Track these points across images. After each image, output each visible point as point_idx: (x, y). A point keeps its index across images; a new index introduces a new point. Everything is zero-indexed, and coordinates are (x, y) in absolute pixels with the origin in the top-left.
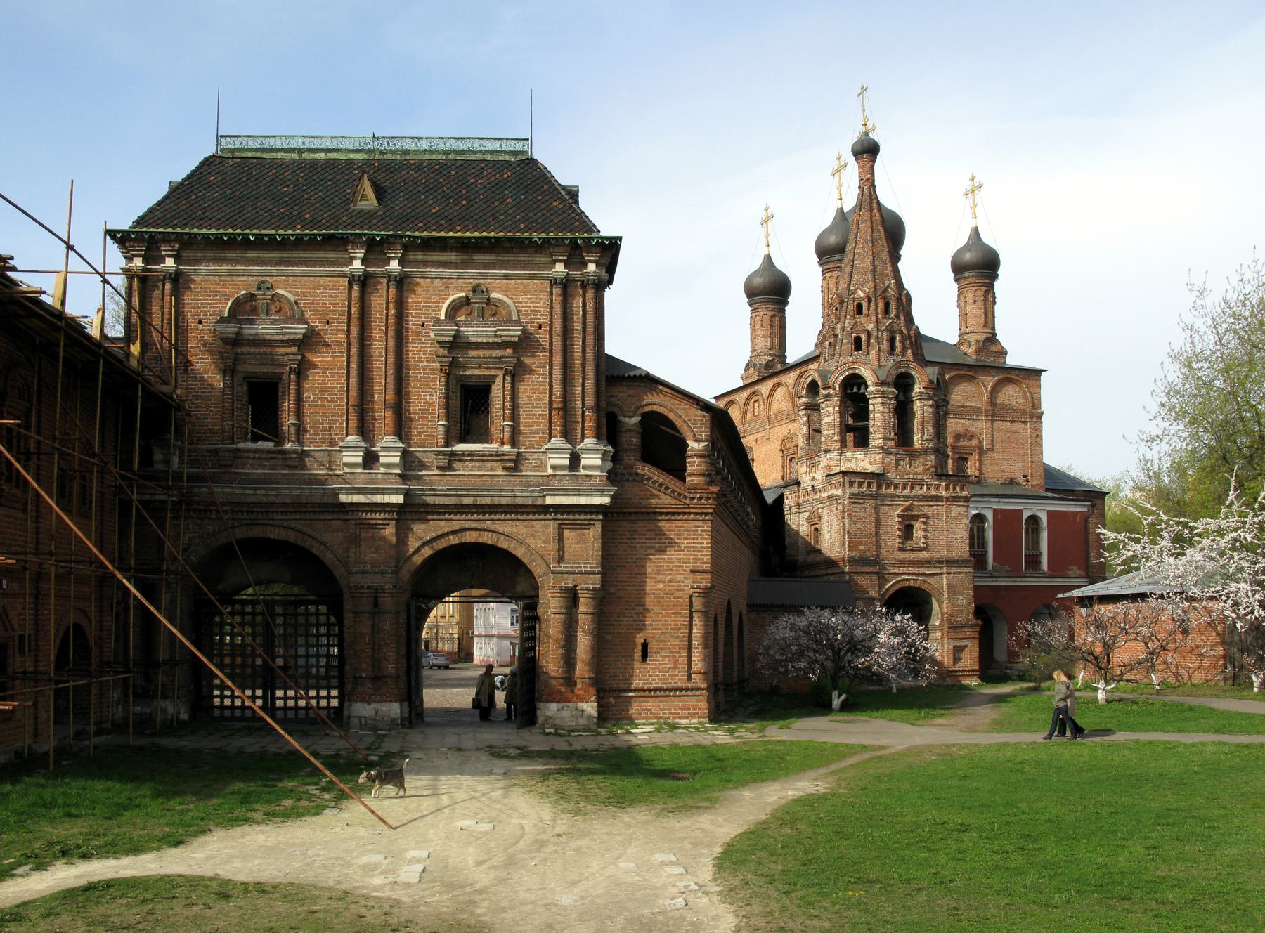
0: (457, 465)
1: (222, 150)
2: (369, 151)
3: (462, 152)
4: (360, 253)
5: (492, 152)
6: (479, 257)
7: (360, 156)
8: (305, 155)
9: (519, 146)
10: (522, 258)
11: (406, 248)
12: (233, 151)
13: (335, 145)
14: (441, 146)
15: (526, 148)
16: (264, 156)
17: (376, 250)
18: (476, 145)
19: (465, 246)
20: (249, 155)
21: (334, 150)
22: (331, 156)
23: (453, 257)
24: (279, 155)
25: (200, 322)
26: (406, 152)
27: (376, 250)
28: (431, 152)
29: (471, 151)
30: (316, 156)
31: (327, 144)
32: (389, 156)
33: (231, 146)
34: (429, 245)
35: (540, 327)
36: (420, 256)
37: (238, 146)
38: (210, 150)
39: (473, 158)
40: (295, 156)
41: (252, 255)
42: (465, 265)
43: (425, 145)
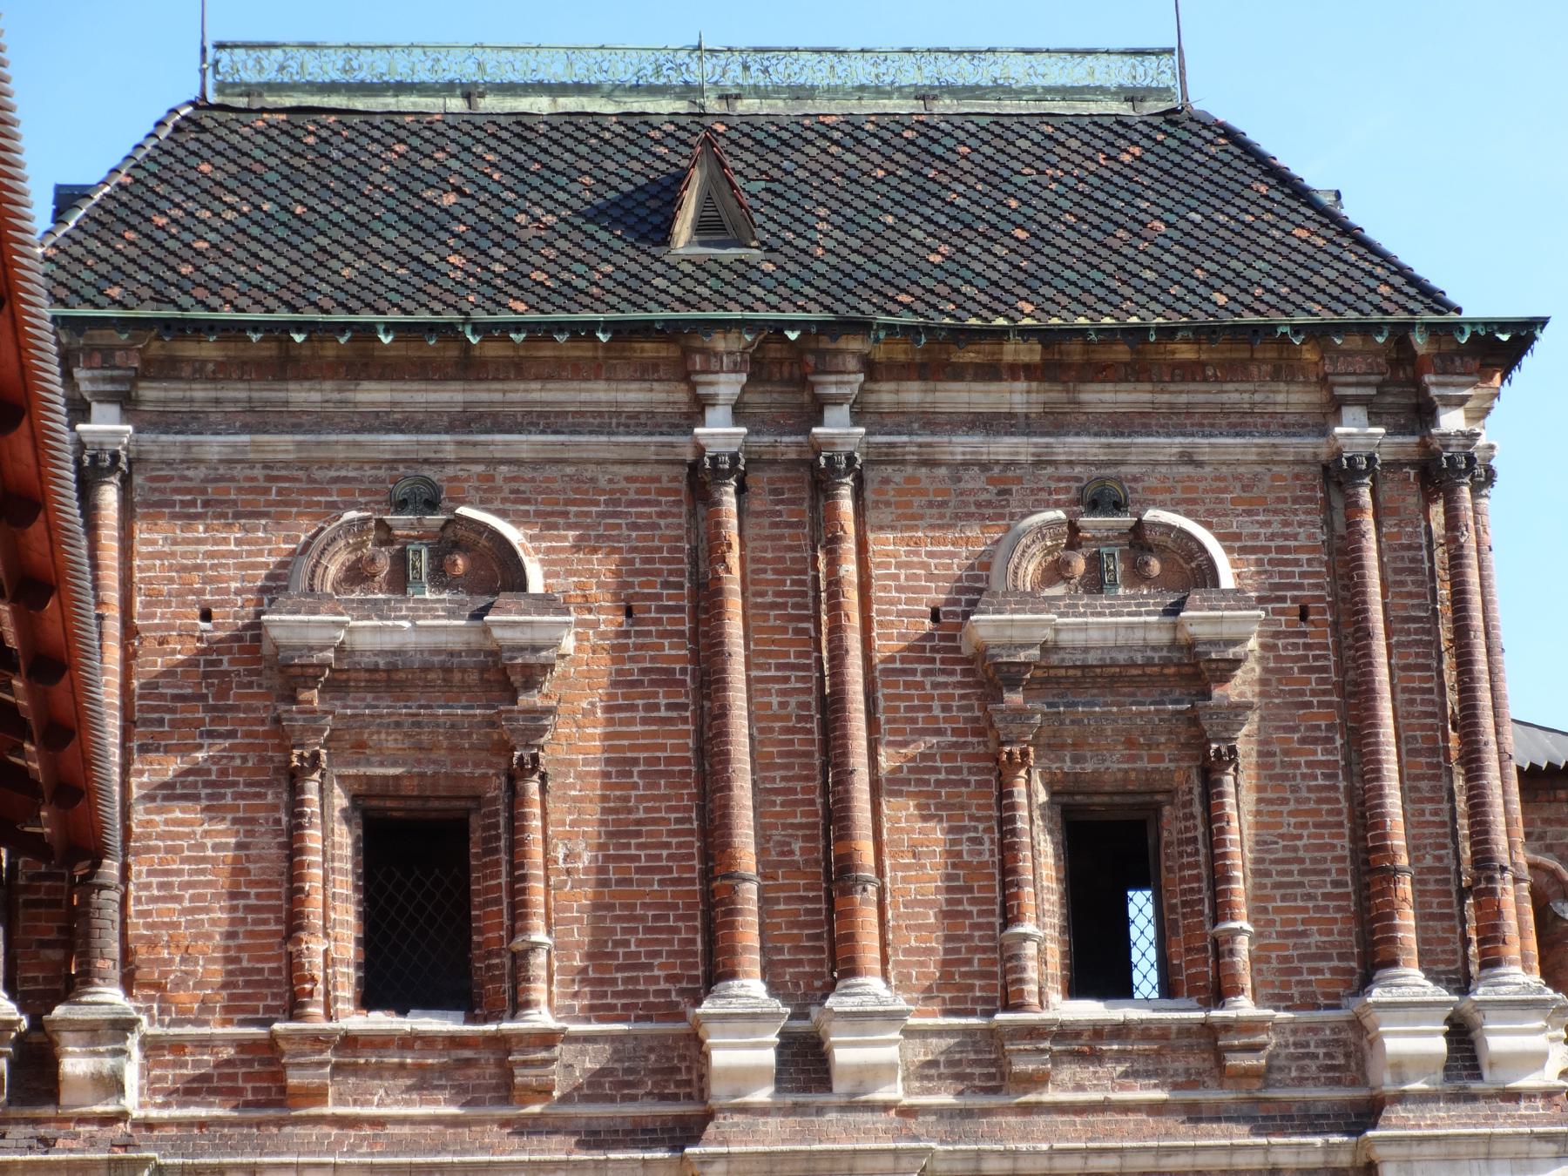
0: (1067, 1072)
1: (221, 88)
2: (689, 91)
3: (974, 91)
4: (728, 386)
5: (1066, 92)
6: (1101, 397)
7: (666, 106)
8: (489, 103)
9: (1149, 73)
10: (1234, 395)
11: (872, 370)
12: (249, 90)
13: (579, 74)
14: (912, 74)
15: (1167, 80)
16: (360, 104)
17: (787, 369)
18: (1018, 71)
19: (1063, 358)
20: (315, 101)
21: (580, 89)
22: (570, 103)
23: (1015, 396)
24: (407, 102)
25: (206, 616)
26: (800, 93)
27: (787, 369)
28: (879, 92)
29: (1002, 90)
30: (524, 104)
31: (555, 70)
32: (746, 105)
33: (250, 76)
34: (940, 352)
35: (1304, 614)
36: (913, 394)
37: (271, 75)
38: (180, 86)
39: (1010, 106)
40: (456, 104)
41: (373, 394)
42: (1054, 422)
43: (861, 71)
